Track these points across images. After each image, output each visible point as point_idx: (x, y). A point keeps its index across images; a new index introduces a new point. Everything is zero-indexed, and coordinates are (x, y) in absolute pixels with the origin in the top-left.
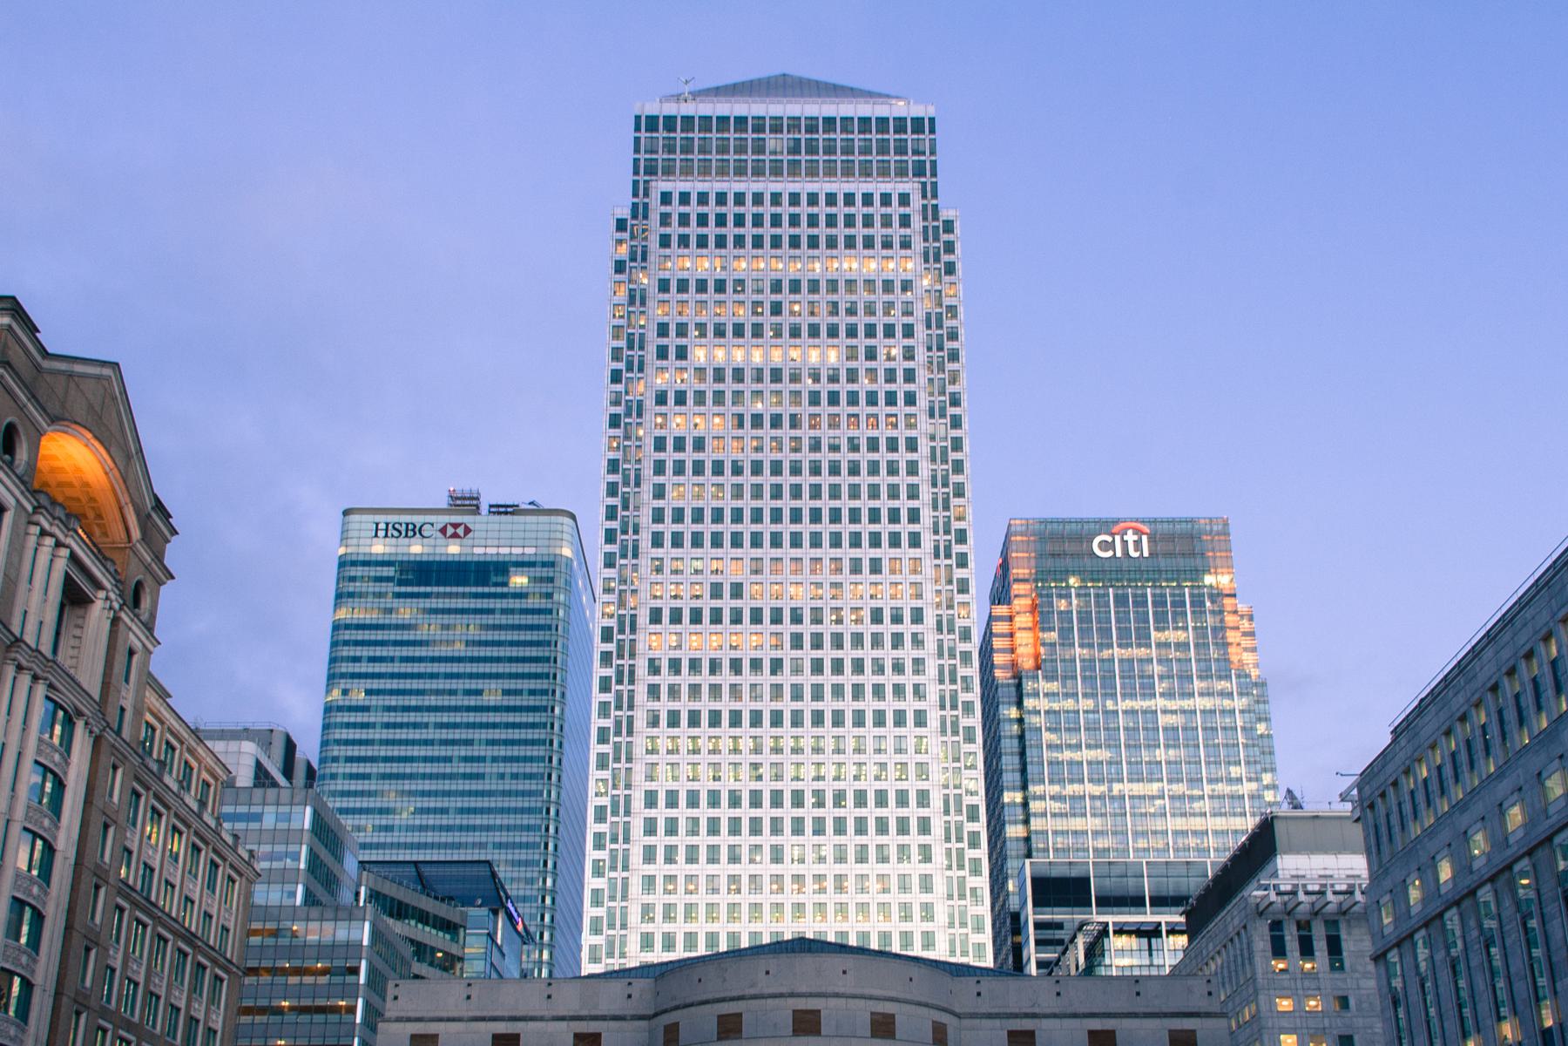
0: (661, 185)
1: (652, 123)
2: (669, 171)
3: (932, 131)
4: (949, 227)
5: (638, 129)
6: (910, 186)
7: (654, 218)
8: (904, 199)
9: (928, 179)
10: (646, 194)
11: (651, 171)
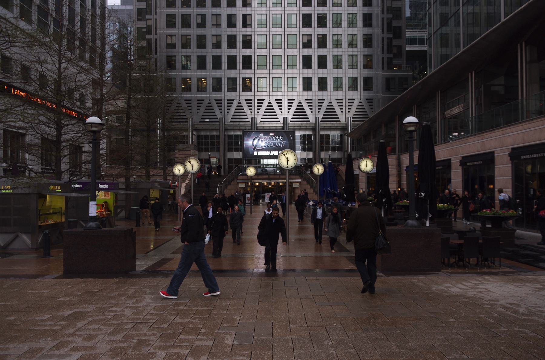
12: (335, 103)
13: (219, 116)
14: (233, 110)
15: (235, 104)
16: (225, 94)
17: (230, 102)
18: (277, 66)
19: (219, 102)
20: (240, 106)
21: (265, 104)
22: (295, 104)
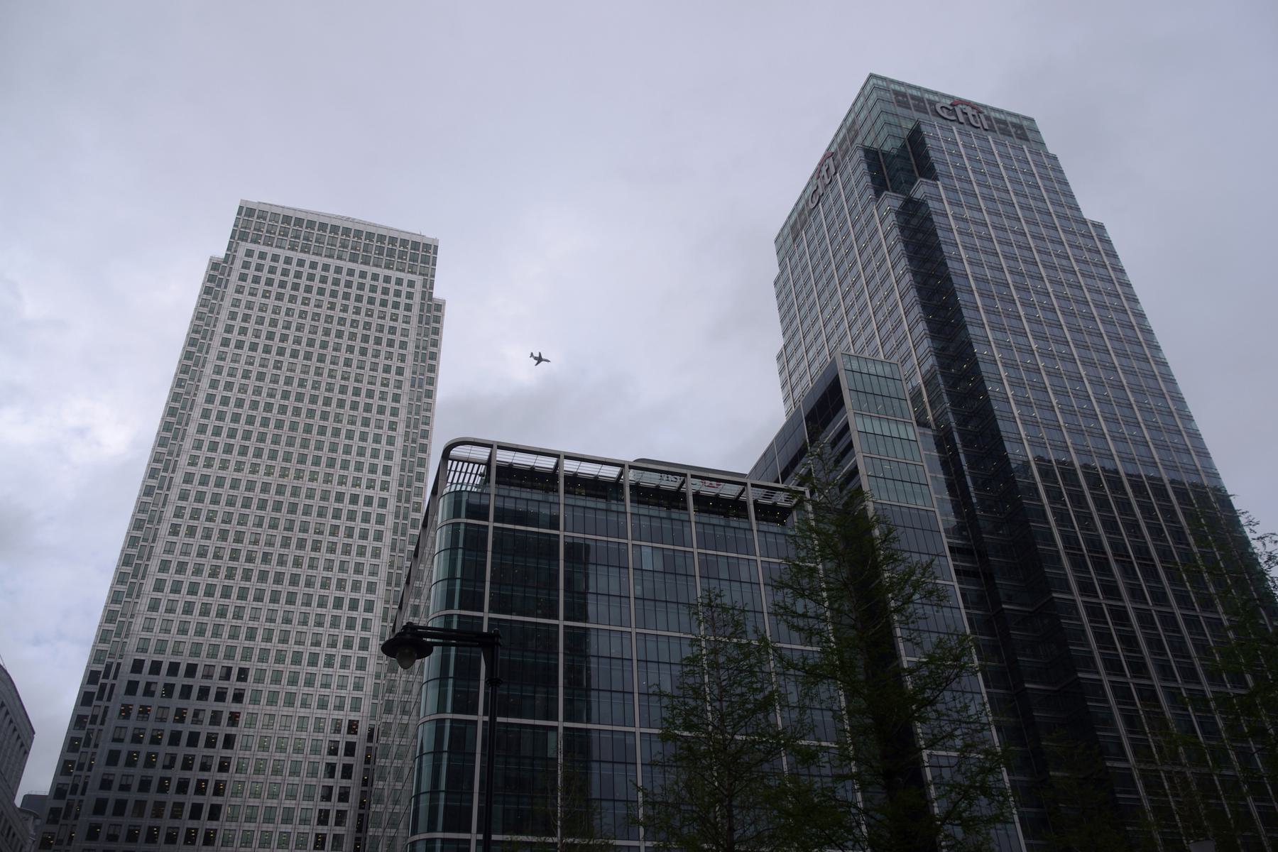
0: (244, 246)
1: (250, 212)
2: (255, 241)
3: (435, 253)
4: (439, 307)
5: (239, 213)
6: (418, 279)
7: (238, 265)
9: (429, 278)
11: (243, 237)
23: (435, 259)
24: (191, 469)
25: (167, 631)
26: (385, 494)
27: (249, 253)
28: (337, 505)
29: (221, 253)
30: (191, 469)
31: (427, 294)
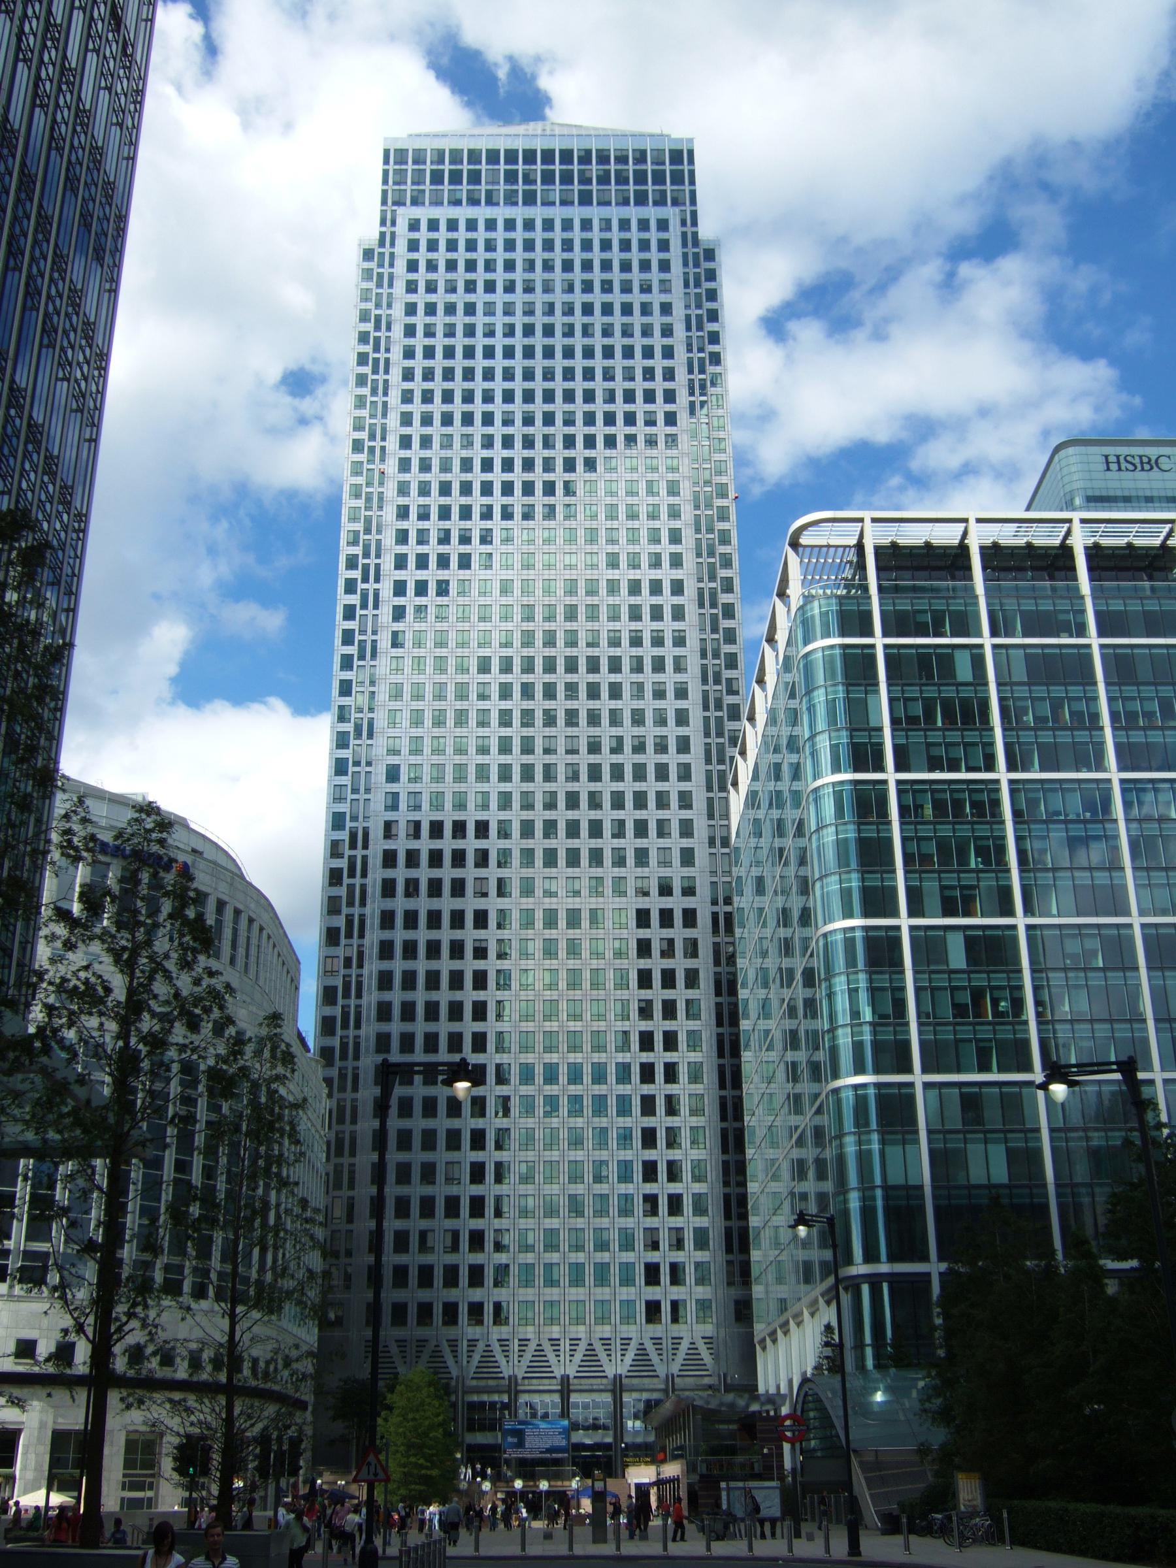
0: (405, 214)
3: (691, 161)
4: (710, 255)
5: (386, 162)
6: (671, 213)
8: (663, 225)
10: (394, 223)
11: (399, 203)
12: (649, 1345)
13: (455, 1372)
14: (477, 1357)
15: (481, 1346)
16: (467, 1330)
17: (473, 1343)
18: (551, 1282)
19: (453, 1344)
20: (488, 1351)
21: (532, 1346)
22: (583, 1346)
23: (692, 173)
24: (400, 575)
25: (418, 808)
26: (678, 574)
27: (414, 226)
28: (611, 600)
29: (371, 231)
30: (400, 575)
31: (691, 239)
